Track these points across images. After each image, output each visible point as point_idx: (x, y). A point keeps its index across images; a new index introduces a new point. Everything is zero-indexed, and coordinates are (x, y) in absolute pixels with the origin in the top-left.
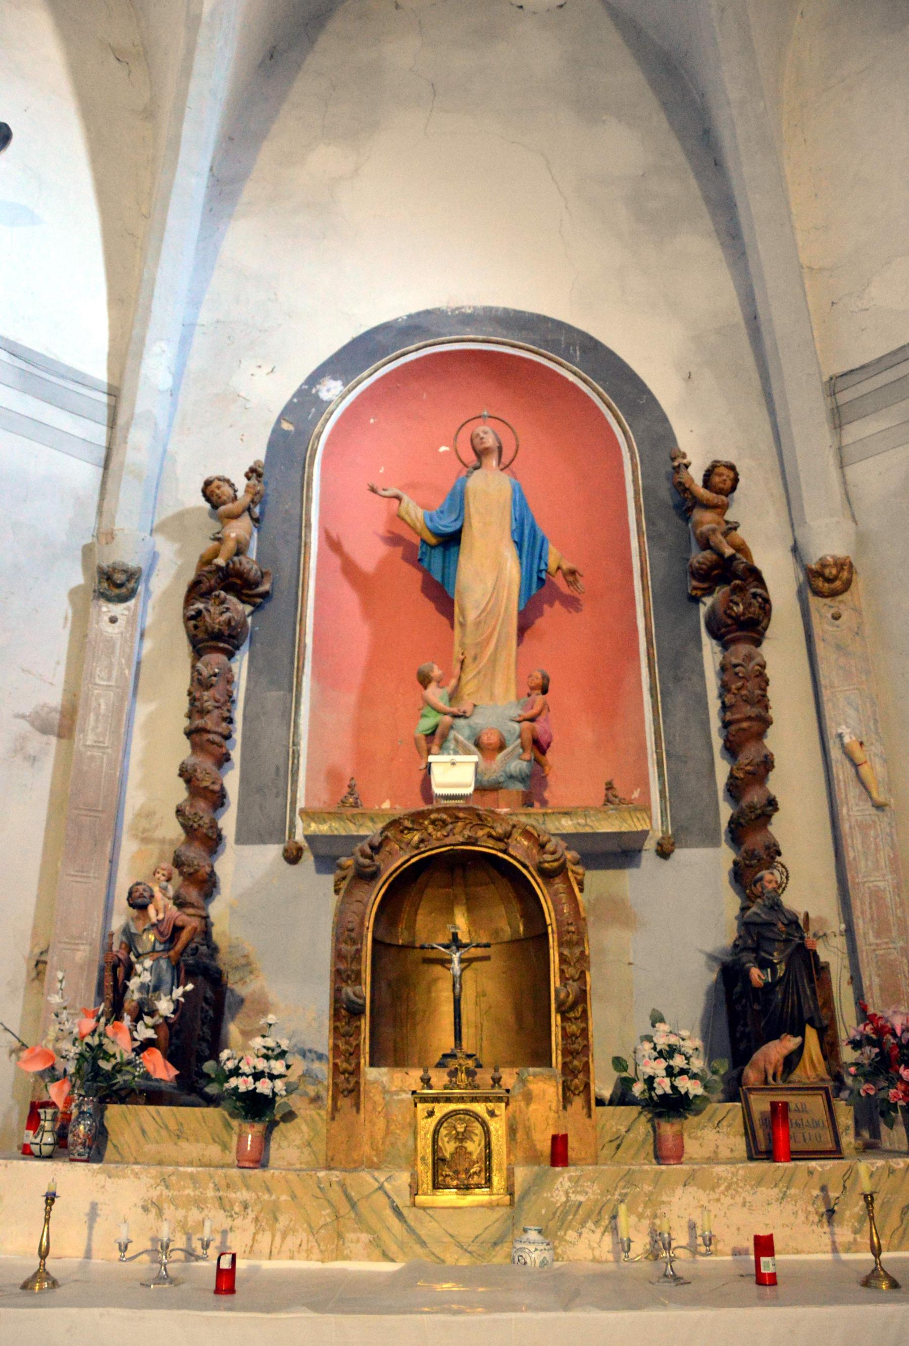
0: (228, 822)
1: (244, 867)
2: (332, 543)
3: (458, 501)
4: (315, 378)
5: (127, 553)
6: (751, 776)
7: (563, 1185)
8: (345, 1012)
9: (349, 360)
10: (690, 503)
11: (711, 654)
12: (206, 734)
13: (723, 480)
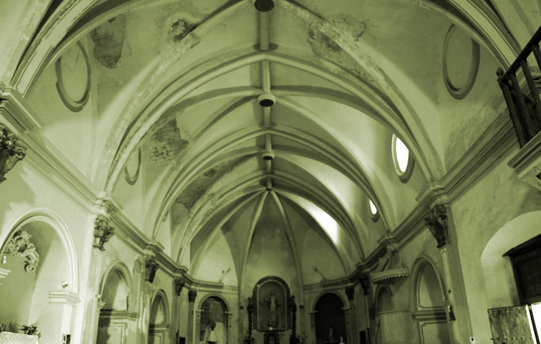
0: (252, 328)
1: (254, 332)
2: (259, 302)
3: (270, 299)
5: (242, 305)
6: (294, 324)
9: (260, 282)
11: (292, 313)
13: (293, 297)
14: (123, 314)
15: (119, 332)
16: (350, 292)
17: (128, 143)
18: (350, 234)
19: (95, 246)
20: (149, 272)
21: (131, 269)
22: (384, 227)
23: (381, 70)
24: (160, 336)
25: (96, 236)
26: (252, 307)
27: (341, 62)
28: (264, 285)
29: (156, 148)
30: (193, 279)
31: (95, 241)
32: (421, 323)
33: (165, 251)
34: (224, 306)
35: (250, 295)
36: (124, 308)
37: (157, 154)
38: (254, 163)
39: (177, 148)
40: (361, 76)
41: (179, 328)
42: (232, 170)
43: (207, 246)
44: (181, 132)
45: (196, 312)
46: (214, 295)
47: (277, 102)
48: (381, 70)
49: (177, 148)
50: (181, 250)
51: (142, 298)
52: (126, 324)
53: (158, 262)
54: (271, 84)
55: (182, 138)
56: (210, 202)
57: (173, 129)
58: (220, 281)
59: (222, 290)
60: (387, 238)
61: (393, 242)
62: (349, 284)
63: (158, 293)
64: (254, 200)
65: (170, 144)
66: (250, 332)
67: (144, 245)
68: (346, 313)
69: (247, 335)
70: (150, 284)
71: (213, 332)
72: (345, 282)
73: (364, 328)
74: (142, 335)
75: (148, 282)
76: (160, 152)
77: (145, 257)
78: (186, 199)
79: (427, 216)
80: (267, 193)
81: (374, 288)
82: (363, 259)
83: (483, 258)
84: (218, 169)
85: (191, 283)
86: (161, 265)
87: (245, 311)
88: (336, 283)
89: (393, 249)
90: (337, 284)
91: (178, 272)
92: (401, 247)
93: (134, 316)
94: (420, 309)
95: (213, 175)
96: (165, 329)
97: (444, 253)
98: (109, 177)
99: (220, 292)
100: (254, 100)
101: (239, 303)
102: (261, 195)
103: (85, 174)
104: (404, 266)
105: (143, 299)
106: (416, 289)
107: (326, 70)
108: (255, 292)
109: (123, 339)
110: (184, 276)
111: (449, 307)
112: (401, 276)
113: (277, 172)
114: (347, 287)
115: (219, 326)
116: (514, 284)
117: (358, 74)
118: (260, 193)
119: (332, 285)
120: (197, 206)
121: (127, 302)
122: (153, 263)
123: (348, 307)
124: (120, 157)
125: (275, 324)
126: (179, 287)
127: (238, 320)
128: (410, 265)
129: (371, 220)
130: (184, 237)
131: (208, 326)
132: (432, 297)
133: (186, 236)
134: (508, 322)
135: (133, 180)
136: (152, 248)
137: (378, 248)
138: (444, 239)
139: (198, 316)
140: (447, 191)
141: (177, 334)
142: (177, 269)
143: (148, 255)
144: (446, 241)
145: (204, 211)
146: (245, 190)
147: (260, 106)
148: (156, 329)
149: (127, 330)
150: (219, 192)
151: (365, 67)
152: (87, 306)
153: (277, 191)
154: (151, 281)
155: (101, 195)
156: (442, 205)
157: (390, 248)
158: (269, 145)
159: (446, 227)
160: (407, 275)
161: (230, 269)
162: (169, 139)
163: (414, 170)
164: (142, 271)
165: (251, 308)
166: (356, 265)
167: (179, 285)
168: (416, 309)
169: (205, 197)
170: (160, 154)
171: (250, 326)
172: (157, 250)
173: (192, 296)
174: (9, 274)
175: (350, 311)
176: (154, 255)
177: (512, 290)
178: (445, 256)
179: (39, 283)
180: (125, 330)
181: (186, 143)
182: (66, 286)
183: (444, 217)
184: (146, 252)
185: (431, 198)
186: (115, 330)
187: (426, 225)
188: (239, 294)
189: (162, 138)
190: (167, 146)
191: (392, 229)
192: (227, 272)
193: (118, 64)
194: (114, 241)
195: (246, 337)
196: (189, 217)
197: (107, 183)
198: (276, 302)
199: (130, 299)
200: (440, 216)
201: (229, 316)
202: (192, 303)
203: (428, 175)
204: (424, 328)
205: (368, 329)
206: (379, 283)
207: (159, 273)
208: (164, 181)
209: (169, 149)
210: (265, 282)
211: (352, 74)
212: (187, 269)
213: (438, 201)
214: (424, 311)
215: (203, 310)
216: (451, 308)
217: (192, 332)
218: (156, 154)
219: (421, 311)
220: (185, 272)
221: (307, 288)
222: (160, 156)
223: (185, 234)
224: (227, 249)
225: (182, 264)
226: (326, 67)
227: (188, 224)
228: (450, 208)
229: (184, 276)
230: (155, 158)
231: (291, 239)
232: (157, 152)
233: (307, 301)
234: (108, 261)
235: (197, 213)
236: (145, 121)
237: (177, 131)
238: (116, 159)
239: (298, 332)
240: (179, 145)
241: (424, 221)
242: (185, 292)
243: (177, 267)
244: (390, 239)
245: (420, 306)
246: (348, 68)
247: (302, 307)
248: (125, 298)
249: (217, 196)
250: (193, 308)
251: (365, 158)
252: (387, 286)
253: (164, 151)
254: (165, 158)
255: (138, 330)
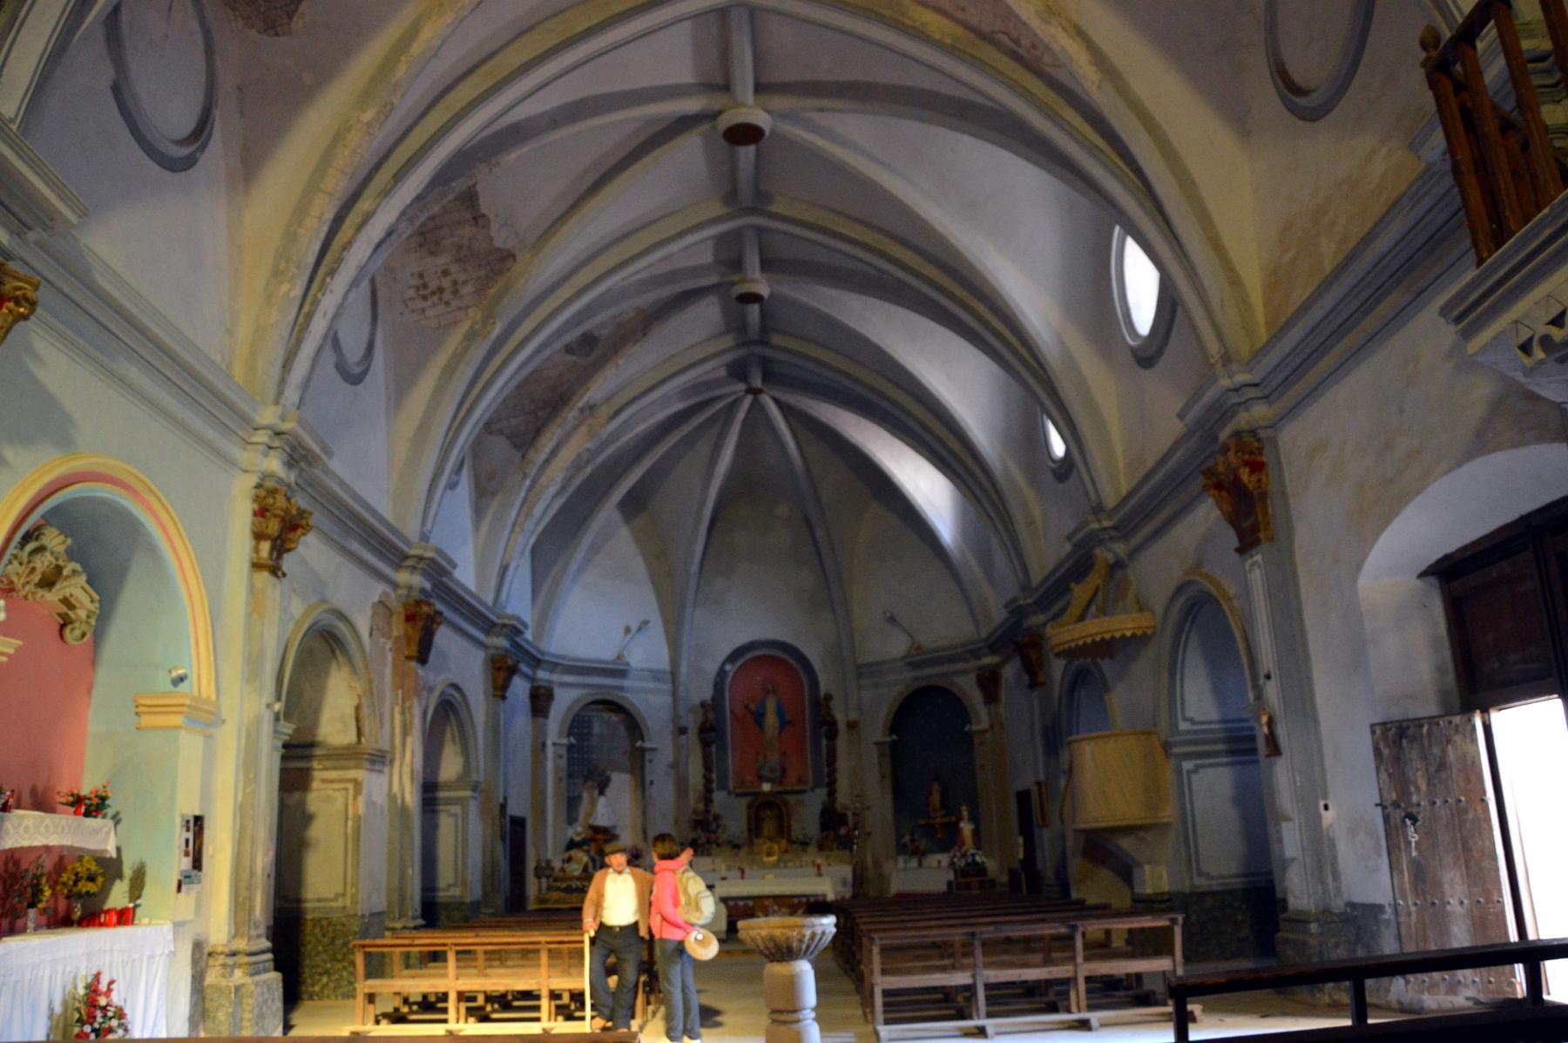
0: (714, 785)
1: (718, 797)
2: (732, 712)
3: (763, 705)
4: (724, 663)
6: (832, 773)
7: (787, 856)
8: (750, 830)
10: (821, 706)
11: (824, 742)
12: (707, 766)
13: (828, 698)
14: (347, 756)
15: (339, 805)
16: (989, 683)
17: (340, 260)
18: (989, 516)
19: (256, 566)
20: (417, 637)
21: (364, 627)
22: (1086, 494)
23: (1080, 34)
24: (455, 815)
25: (258, 536)
26: (712, 729)
27: (963, 9)
28: (744, 664)
29: (421, 276)
30: (543, 653)
31: (257, 550)
32: (1187, 765)
33: (457, 574)
34: (634, 727)
35: (707, 694)
36: (350, 737)
37: (425, 291)
38: (708, 312)
39: (483, 273)
40: (1022, 51)
41: (505, 791)
42: (645, 335)
43: (579, 556)
44: (494, 225)
45: (554, 744)
46: (600, 697)
47: (773, 132)
48: (1080, 34)
49: (483, 273)
50: (504, 570)
51: (397, 709)
52: (357, 784)
53: (439, 606)
54: (756, 78)
55: (498, 243)
56: (583, 429)
57: (469, 217)
58: (619, 657)
59: (625, 683)
60: (1095, 526)
61: (1111, 538)
62: (988, 660)
63: (443, 693)
64: (710, 421)
65: (459, 260)
66: (708, 800)
67: (398, 558)
68: (976, 741)
69: (701, 807)
70: (421, 671)
71: (602, 800)
72: (976, 654)
73: (1026, 781)
74: (404, 811)
75: (413, 664)
76: (433, 286)
77: (403, 592)
78: (514, 422)
79: (1209, 463)
80: (749, 399)
81: (1057, 669)
82: (1025, 587)
83: (1363, 582)
84: (604, 332)
85: (537, 662)
86: (448, 613)
87: (692, 740)
88: (952, 656)
89: (1111, 558)
90: (952, 659)
91: (498, 635)
92: (1132, 554)
93: (380, 760)
94: (1183, 726)
95: (592, 350)
96: (468, 793)
97: (1256, 570)
98: (287, 365)
99: (621, 688)
100: (705, 127)
101: (676, 718)
102: (732, 408)
103: (218, 358)
104: (1142, 607)
105: (403, 713)
106: (1173, 668)
107: (920, 35)
108: (718, 687)
109: (350, 823)
110: (514, 644)
111: (1264, 719)
112: (1134, 635)
113: (777, 339)
114: (980, 668)
115: (621, 782)
116: (1447, 653)
117: (1014, 47)
118: (730, 399)
119: (938, 661)
120: (548, 441)
121: (358, 720)
122: (425, 609)
123: (985, 725)
124: (316, 302)
125: (777, 774)
126: (502, 675)
127: (674, 766)
128: (1158, 607)
129: (1049, 475)
130: (512, 532)
131: (590, 783)
132: (1219, 691)
133: (517, 529)
134: (1424, 757)
135: (357, 370)
136: (421, 565)
137: (1069, 555)
138: (1255, 529)
139: (560, 757)
140: (1266, 392)
141: (503, 807)
142: (494, 624)
143: (410, 588)
144: (1261, 536)
145: (566, 456)
146: (685, 393)
147: (721, 142)
148: (442, 794)
149: (361, 799)
150: (608, 399)
151: (1035, 23)
152: (244, 735)
153: (779, 395)
154: (422, 659)
155: (268, 415)
156: (1253, 433)
157: (1104, 555)
158: (753, 260)
159: (1263, 496)
160: (1149, 632)
161: (646, 623)
162: (459, 247)
163: (1176, 326)
164: (395, 633)
165: (710, 733)
166: (1006, 606)
167: (502, 671)
168: (1174, 725)
169: (570, 415)
170: (433, 293)
171: (708, 780)
172: (438, 570)
173: (540, 700)
174: (18, 650)
175: (989, 736)
176: (428, 586)
177: (1440, 670)
178: (1257, 578)
179: (102, 675)
180: (355, 798)
181: (507, 257)
182: (182, 679)
183: (1257, 467)
184: (403, 577)
185: (1221, 412)
186: (328, 800)
187: (1205, 488)
188: (674, 693)
189: (437, 243)
190: (453, 268)
191: (1110, 501)
192: (639, 629)
193: (297, 24)
194: (311, 550)
195: (695, 811)
196: (525, 476)
197: (282, 382)
198: (780, 712)
199: (365, 711)
200: (1246, 463)
201: (648, 756)
202: (541, 720)
203: (1213, 346)
204: (1194, 778)
205: (1038, 784)
206: (1070, 654)
207: (444, 638)
208: (449, 371)
209: (461, 277)
210: (749, 656)
211: (998, 45)
212: (526, 626)
213: (1243, 420)
214: (1196, 732)
215: (573, 741)
216: (1270, 723)
217: (544, 801)
218: (422, 292)
219: (1188, 732)
220: (519, 632)
221: (868, 671)
222: (435, 298)
223: (514, 525)
224: (639, 566)
225: (509, 611)
226: (917, 24)
227: (523, 494)
228: (1273, 441)
229: (514, 644)
230: (420, 304)
231: (820, 533)
232: (425, 286)
233: (868, 710)
234: (297, 608)
235: (547, 461)
236: (386, 193)
237: (481, 222)
238: (306, 309)
239: (843, 796)
240: (489, 263)
241: (1201, 477)
242: (519, 688)
243: (494, 618)
244: (1105, 529)
245: (1185, 719)
246: (985, 28)
247: (852, 726)
248: (350, 711)
249: (605, 411)
250: (545, 734)
251: (1032, 297)
252: (1092, 665)
253: (446, 283)
254: (447, 303)
255: (392, 798)
